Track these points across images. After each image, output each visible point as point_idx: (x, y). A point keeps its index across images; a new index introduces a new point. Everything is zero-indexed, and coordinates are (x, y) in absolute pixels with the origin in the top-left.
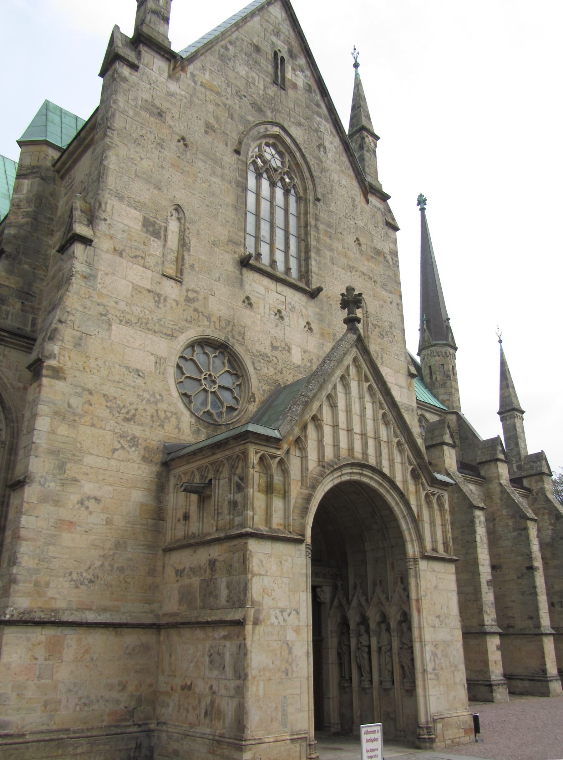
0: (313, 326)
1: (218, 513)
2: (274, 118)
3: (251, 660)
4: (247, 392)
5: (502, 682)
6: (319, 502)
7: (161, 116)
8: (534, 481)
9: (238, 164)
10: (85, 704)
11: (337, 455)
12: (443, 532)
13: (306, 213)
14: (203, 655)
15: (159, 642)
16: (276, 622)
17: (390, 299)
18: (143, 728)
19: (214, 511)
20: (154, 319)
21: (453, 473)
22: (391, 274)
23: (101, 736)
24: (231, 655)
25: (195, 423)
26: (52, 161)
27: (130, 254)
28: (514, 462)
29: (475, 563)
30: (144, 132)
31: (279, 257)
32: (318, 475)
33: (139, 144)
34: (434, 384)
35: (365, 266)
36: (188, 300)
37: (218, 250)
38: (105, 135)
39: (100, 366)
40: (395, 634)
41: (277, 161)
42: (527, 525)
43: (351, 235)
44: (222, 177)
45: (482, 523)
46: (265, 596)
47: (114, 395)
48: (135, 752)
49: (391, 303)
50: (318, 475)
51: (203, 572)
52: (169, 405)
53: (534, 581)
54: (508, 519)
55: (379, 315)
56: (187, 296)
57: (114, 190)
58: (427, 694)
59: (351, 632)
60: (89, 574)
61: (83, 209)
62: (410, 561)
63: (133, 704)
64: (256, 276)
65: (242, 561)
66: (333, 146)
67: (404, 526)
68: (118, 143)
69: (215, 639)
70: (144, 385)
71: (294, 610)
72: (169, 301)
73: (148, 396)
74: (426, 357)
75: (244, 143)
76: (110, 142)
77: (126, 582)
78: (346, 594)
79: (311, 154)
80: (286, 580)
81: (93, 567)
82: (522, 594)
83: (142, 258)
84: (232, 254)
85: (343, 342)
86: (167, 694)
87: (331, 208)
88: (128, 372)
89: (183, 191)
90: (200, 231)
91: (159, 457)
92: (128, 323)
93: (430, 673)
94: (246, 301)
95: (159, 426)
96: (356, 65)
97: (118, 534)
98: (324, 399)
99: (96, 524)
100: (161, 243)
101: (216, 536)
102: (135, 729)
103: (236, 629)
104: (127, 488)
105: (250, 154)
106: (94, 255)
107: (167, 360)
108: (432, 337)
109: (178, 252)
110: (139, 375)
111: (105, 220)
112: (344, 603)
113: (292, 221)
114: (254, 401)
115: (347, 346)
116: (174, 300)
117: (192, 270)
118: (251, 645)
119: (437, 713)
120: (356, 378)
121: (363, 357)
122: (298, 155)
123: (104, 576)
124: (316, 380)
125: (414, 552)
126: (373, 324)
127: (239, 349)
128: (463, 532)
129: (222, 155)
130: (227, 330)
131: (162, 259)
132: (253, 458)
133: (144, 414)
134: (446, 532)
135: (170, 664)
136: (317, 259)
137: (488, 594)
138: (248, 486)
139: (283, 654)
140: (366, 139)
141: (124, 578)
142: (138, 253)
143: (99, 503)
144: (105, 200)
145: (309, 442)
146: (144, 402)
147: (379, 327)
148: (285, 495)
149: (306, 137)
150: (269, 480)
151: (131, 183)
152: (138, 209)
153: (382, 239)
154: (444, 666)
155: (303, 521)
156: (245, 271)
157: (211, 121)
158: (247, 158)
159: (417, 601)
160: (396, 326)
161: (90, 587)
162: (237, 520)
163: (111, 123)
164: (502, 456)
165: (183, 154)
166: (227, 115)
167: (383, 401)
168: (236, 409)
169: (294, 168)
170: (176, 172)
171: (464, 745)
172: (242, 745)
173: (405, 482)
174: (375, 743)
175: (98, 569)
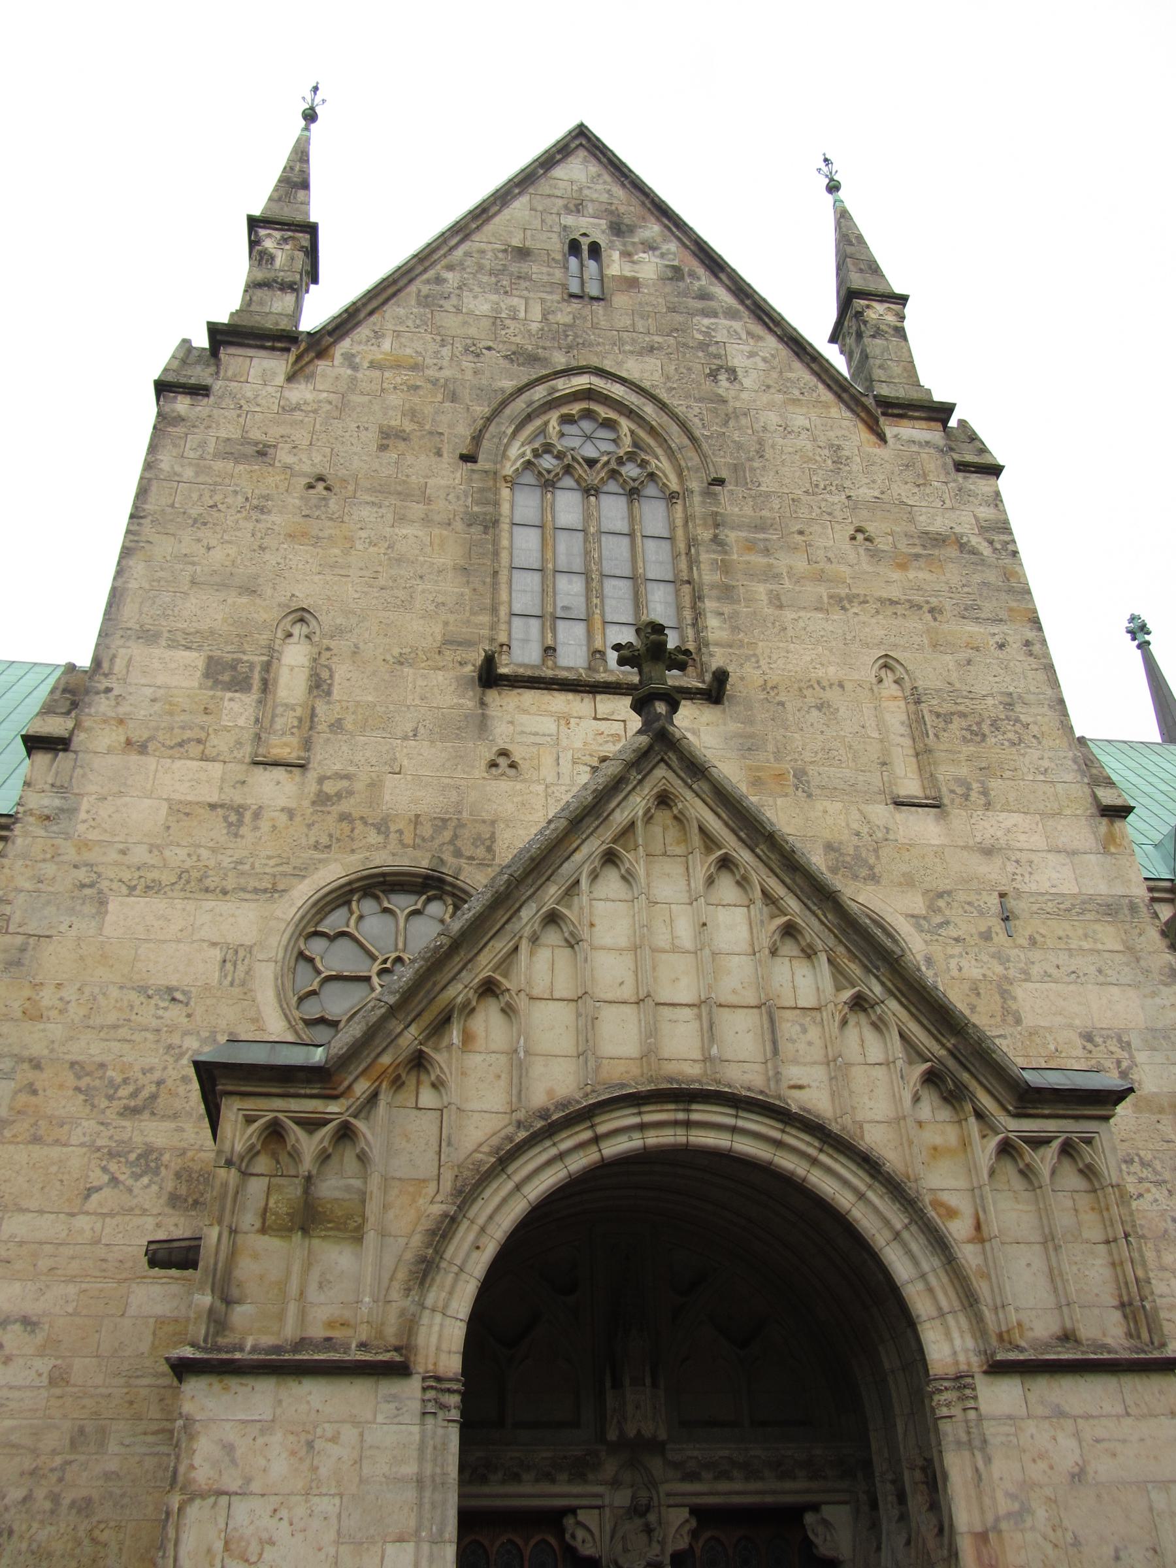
17: (997, 638)
20: (225, 864)
22: (992, 577)
30: (218, 498)
36: (322, 800)
37: (411, 671)
39: (68, 999)
44: (426, 520)
47: (98, 1059)
55: (958, 686)
64: (529, 697)
72: (266, 814)
73: (195, 1045)
79: (688, 396)
80: (327, 1505)
83: (199, 741)
84: (453, 669)
88: (142, 999)
89: (316, 578)
90: (361, 645)
92: (152, 888)
96: (833, 187)
99: (19, 1388)
107: (255, 949)
110: (174, 999)
116: (283, 810)
117: (336, 733)
122: (649, 410)
123: (30, 1527)
126: (938, 715)
130: (437, 842)
133: (181, 1090)
142: (188, 734)
144: (113, 651)
147: (963, 715)
153: (948, 504)
156: (492, 696)
160: (1030, 698)
165: (318, 507)
169: (651, 442)
175: (13, 1511)
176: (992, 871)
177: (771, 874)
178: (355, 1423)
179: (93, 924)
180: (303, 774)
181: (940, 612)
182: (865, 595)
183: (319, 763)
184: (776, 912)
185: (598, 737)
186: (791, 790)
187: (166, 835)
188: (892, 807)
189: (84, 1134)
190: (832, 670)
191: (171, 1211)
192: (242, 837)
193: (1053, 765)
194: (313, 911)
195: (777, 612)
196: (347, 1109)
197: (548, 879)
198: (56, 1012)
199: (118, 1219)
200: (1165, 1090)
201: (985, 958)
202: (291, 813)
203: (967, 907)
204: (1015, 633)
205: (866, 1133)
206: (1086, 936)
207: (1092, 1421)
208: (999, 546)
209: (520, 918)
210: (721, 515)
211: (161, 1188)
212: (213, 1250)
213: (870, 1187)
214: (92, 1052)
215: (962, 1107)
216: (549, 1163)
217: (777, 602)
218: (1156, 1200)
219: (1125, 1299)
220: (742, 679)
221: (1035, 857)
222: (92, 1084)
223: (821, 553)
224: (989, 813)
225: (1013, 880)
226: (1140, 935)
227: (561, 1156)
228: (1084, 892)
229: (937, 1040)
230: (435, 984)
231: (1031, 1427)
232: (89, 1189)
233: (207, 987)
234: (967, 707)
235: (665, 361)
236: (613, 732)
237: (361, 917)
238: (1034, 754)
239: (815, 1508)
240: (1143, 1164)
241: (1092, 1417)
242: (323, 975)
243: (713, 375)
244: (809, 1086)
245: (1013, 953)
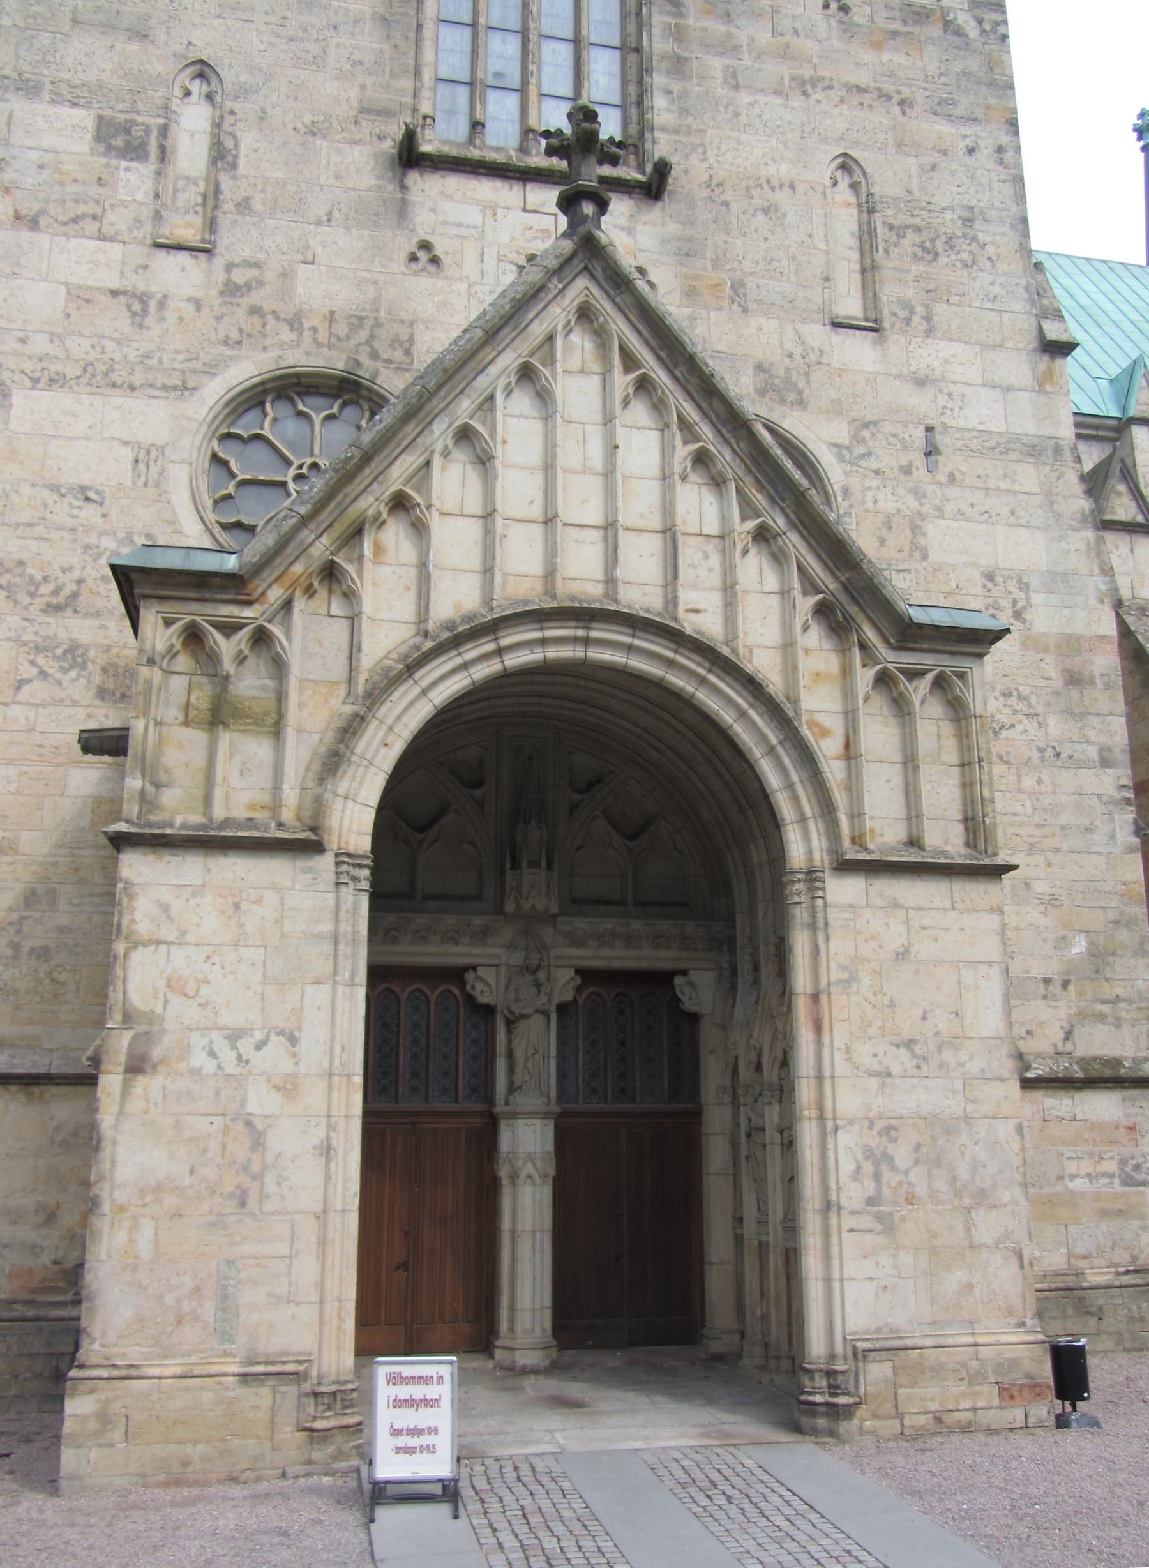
3: (114, 1163)
12: (964, 785)
16: (210, 1066)
17: (968, 141)
20: (131, 358)
36: (231, 290)
37: (325, 144)
47: (17, 556)
55: (917, 194)
56: (229, 280)
64: (453, 182)
70: (101, 520)
71: (281, 1033)
72: (172, 304)
73: (113, 545)
77: (54, 981)
80: (256, 954)
83: (94, 217)
84: (371, 143)
88: (56, 497)
89: (216, 22)
90: (269, 109)
97: (34, 873)
100: (147, 169)
107: (167, 451)
109: (207, 181)
110: (87, 499)
116: (189, 300)
117: (243, 214)
118: (115, 1127)
119: (878, 1330)
121: (613, 300)
125: (810, 852)
126: (891, 228)
130: (353, 342)
131: (152, 207)
134: (971, 784)
139: (229, 1147)
141: (50, 973)
142: (82, 209)
147: (918, 229)
154: (921, 1190)
156: (414, 178)
159: (815, 997)
160: (993, 215)
174: (424, 1411)
176: (922, 403)
177: (688, 398)
178: (276, 889)
180: (210, 260)
181: (911, 106)
182: (831, 79)
183: (226, 248)
184: (689, 437)
185: (527, 232)
186: (726, 303)
187: (66, 322)
188: (829, 327)
189: (10, 629)
190: (784, 167)
191: (101, 703)
192: (148, 328)
193: (1003, 292)
194: (226, 411)
195: (732, 94)
196: (262, 614)
197: (462, 392)
199: (51, 709)
200: (1054, 631)
201: (901, 492)
202: (198, 304)
203: (891, 439)
204: (989, 136)
205: (755, 657)
206: (1005, 476)
207: (921, 913)
208: (987, 27)
209: (432, 432)
211: (89, 681)
212: (141, 739)
213: (751, 706)
215: (847, 638)
216: (454, 671)
217: (733, 81)
218: (1026, 731)
219: (969, 814)
220: (686, 172)
222: (13, 581)
223: (788, 22)
224: (929, 341)
225: (942, 414)
226: (1059, 478)
227: (465, 666)
228: (1011, 430)
229: (833, 574)
230: (346, 496)
231: (868, 914)
232: (19, 681)
233: (121, 487)
234: (923, 220)
236: (542, 227)
237: (275, 420)
238: (985, 278)
239: (684, 973)
240: (1020, 698)
241: (922, 909)
242: (238, 479)
244: (705, 611)
245: (930, 489)
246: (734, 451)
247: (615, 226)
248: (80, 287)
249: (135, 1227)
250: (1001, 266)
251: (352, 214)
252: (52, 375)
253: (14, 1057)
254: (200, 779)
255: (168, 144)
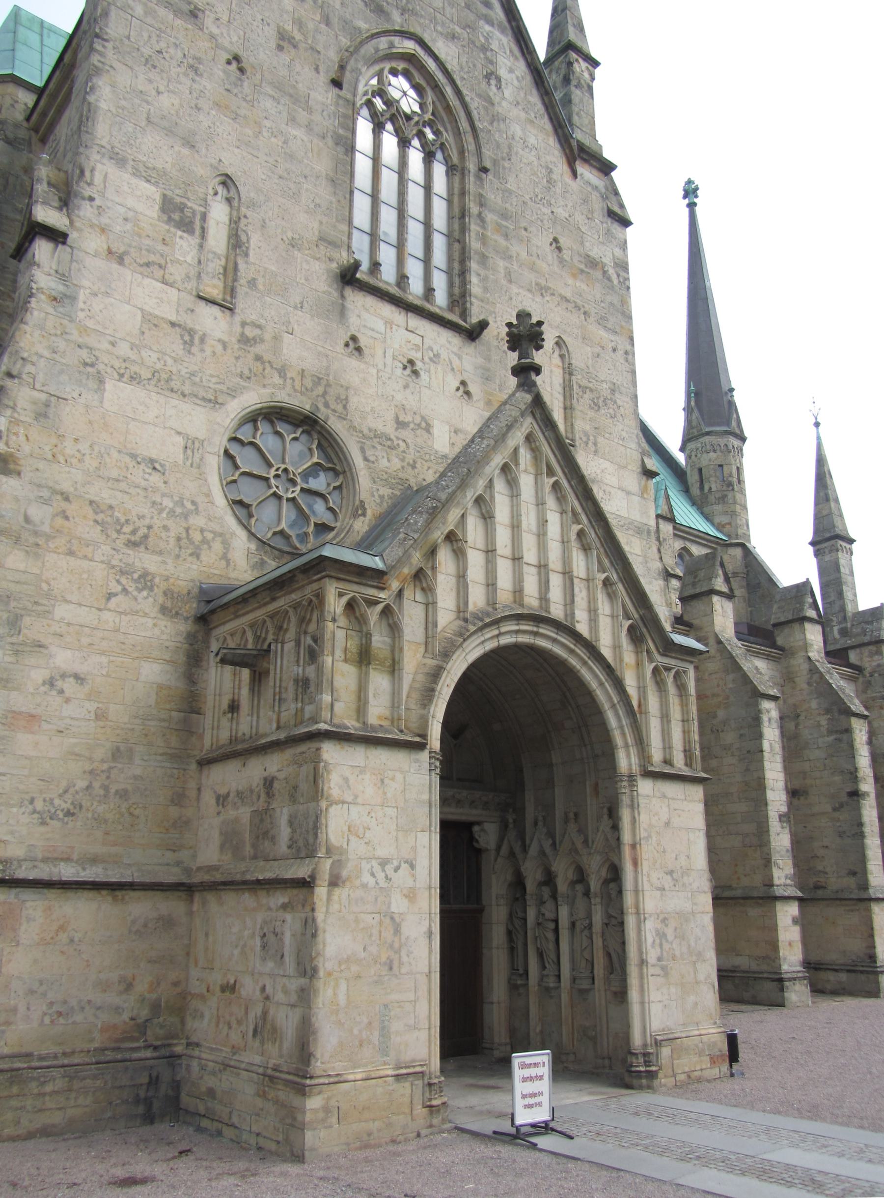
0: (472, 388)
1: (280, 699)
2: (405, 25)
4: (351, 498)
5: (800, 975)
6: (456, 679)
7: (196, 17)
8: (866, 654)
9: (337, 104)
10: (60, 1014)
11: (492, 602)
12: (684, 732)
13: (463, 193)
14: (253, 936)
15: (190, 914)
16: (371, 881)
17: (613, 344)
18: (163, 1052)
19: (274, 696)
20: (183, 373)
21: (727, 640)
22: (616, 300)
23: (88, 1064)
24: (293, 935)
25: (257, 550)
26: (25, 111)
27: (138, 260)
28: (834, 624)
29: (761, 785)
30: (163, 45)
31: (414, 270)
32: (455, 635)
33: (155, 67)
34: (707, 498)
35: (568, 285)
36: (244, 340)
37: (299, 255)
38: (92, 49)
39: (83, 452)
40: (598, 900)
41: (411, 101)
42: (850, 725)
43: (545, 233)
44: (309, 127)
45: (773, 721)
46: (353, 839)
47: (108, 502)
48: (148, 1090)
49: (614, 350)
50: (455, 635)
51: (255, 797)
52: (209, 519)
53: (860, 816)
54: (819, 714)
57: (109, 147)
58: (647, 1000)
59: (528, 897)
60: (66, 802)
61: (53, 181)
62: (622, 781)
63: (145, 1013)
64: (370, 301)
65: (311, 778)
66: (514, 76)
67: (612, 722)
68: (116, 64)
69: (270, 909)
70: (163, 485)
72: (210, 342)
73: (171, 505)
74: (693, 454)
75: (349, 68)
76: (99, 61)
78: (522, 836)
79: (472, 90)
80: (392, 812)
81: (72, 790)
82: (840, 836)
83: (160, 266)
85: (508, 407)
86: (202, 997)
87: (508, 186)
88: (134, 463)
89: (236, 151)
90: (267, 221)
91: (192, 608)
92: (135, 379)
93: (653, 966)
94: (351, 343)
95: (191, 555)
97: (118, 735)
98: (470, 505)
99: (77, 719)
100: (195, 241)
101: (274, 738)
102: (149, 1053)
103: (299, 894)
104: (133, 659)
105: (361, 89)
106: (71, 261)
107: (205, 443)
108: (703, 420)
110: (154, 468)
111: (91, 199)
112: (517, 849)
113: (439, 209)
114: (364, 515)
115: (513, 414)
116: (219, 341)
118: (325, 921)
119: (663, 1030)
120: (531, 470)
121: (543, 434)
122: (449, 90)
124: (454, 470)
125: (630, 765)
126: (580, 387)
127: (336, 425)
128: (741, 735)
129: (309, 88)
130: (315, 393)
131: (197, 269)
132: (335, 604)
133: (164, 535)
134: (689, 732)
135: (207, 949)
136: (482, 272)
137: (781, 835)
138: (323, 651)
139: (383, 934)
140: (576, 65)
142: (152, 258)
143: (82, 684)
144: (92, 164)
145: (441, 578)
146: (164, 515)
147: (591, 390)
148: (394, 668)
149: (465, 60)
150: (364, 642)
151: (139, 135)
152: (153, 180)
153: (601, 239)
154: (677, 953)
155: (425, 712)
156: (348, 291)
157: (288, 28)
158: (354, 95)
159: (633, 846)
160: (623, 389)
161: (67, 823)
162: (309, 710)
163: (101, 29)
164: (812, 613)
165: (236, 85)
166: (318, 18)
167: (579, 509)
168: (333, 529)
170: (222, 116)
171: (709, 1081)
172: (304, 1086)
173: (616, 647)
174: (537, 1083)
175: (81, 794)
178: (402, 772)
179: (96, 397)
189: (103, 555)
196: (389, 597)
198: (76, 460)
199: (129, 617)
210: (485, 198)
212: (330, 670)
214: (103, 495)
219: (687, 748)
221: (613, 491)
222: (106, 519)
231: (654, 801)
233: (176, 464)
235: (461, 51)
237: (262, 433)
239: (478, 823)
242: (242, 470)
243: (488, 76)
246: (596, 533)
247: (453, 352)
248: (151, 314)
249: (337, 986)
250: (627, 421)
251: (315, 307)
252: (132, 374)
253: (106, 869)
254: (353, 697)
255: (206, 226)
